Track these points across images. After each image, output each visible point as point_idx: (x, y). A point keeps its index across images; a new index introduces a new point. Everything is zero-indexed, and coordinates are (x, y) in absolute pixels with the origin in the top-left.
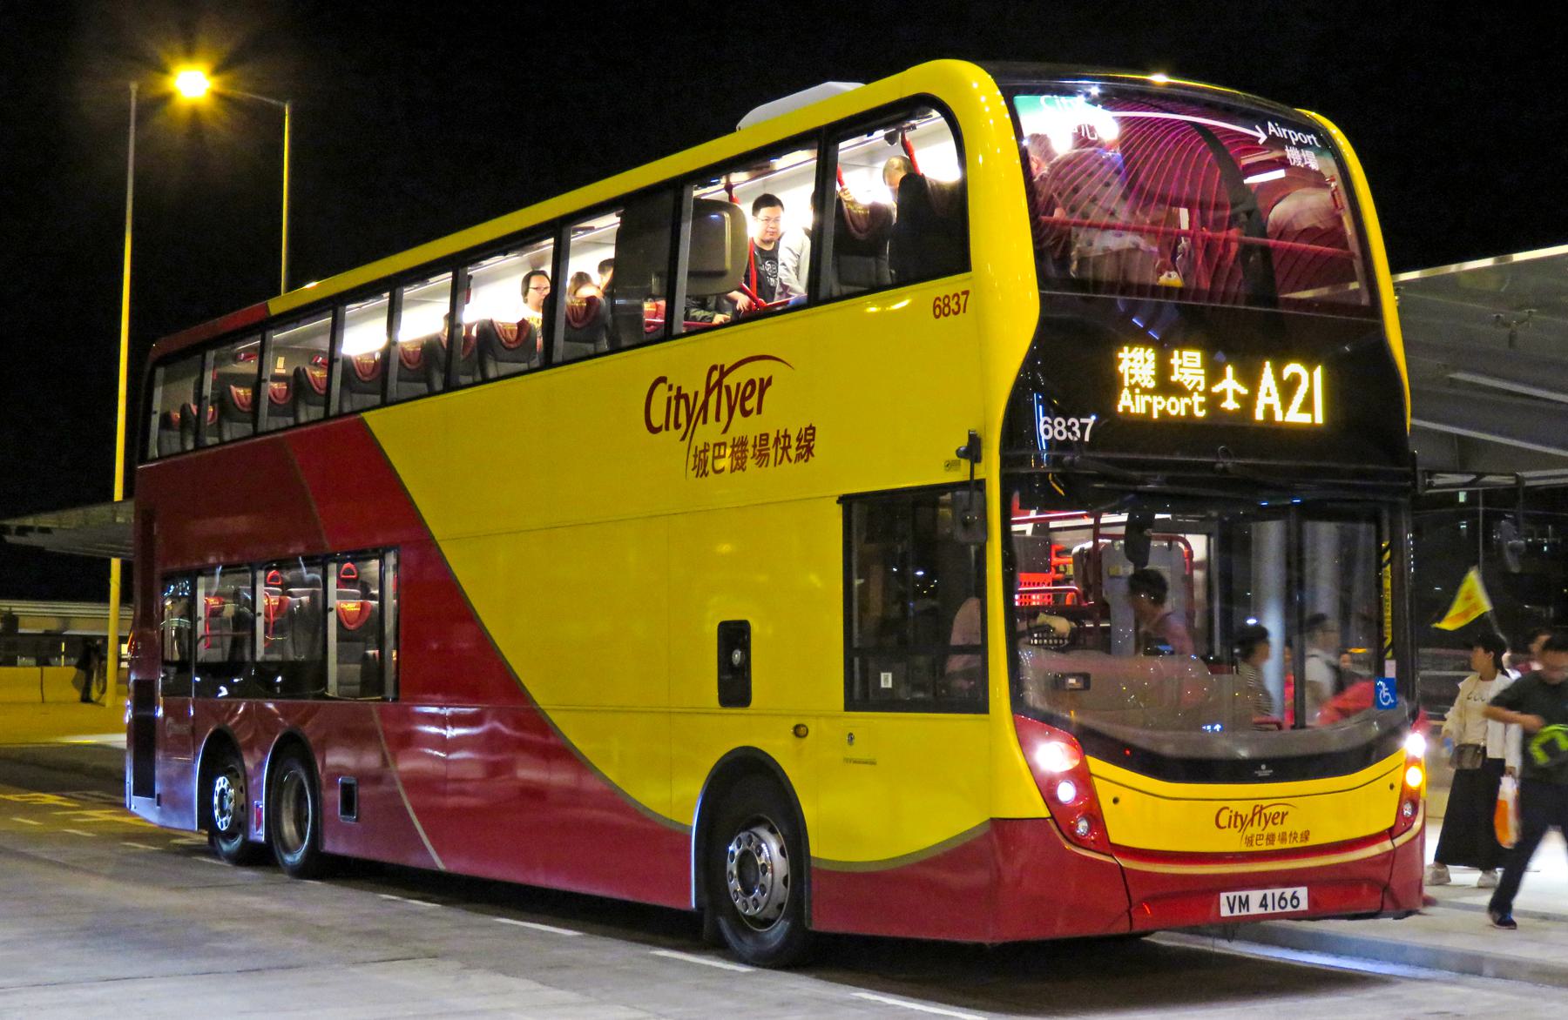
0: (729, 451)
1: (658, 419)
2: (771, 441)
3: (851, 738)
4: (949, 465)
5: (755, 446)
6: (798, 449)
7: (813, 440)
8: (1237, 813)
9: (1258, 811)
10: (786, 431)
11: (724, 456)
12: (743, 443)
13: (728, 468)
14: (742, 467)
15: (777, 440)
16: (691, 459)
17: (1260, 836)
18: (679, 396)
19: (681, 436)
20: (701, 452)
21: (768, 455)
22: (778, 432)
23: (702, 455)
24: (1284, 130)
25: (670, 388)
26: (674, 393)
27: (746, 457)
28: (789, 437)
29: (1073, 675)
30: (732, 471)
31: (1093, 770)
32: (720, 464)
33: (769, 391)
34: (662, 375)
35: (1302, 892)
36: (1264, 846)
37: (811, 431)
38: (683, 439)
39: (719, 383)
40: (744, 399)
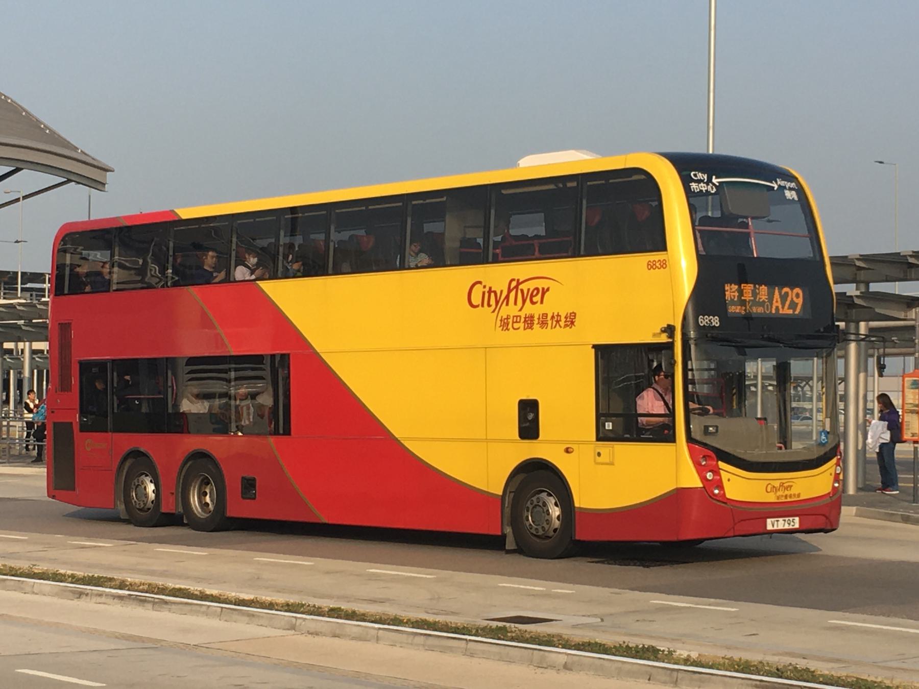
0: (523, 320)
1: (476, 300)
2: (549, 318)
3: (599, 454)
4: (654, 335)
5: (539, 319)
6: (565, 322)
7: (575, 318)
8: (774, 487)
9: (782, 485)
10: (558, 313)
11: (520, 322)
12: (532, 317)
13: (522, 328)
14: (531, 328)
15: (553, 317)
16: (499, 323)
17: (782, 496)
18: (490, 291)
19: (492, 310)
20: (505, 319)
21: (547, 324)
22: (553, 313)
23: (506, 321)
24: (783, 182)
25: (485, 287)
26: (487, 289)
27: (533, 323)
28: (560, 316)
29: (711, 426)
30: (525, 329)
31: (720, 467)
32: (516, 325)
33: (547, 293)
34: (480, 280)
35: (797, 519)
36: (783, 500)
37: (573, 315)
38: (494, 311)
39: (516, 287)
40: (532, 296)
